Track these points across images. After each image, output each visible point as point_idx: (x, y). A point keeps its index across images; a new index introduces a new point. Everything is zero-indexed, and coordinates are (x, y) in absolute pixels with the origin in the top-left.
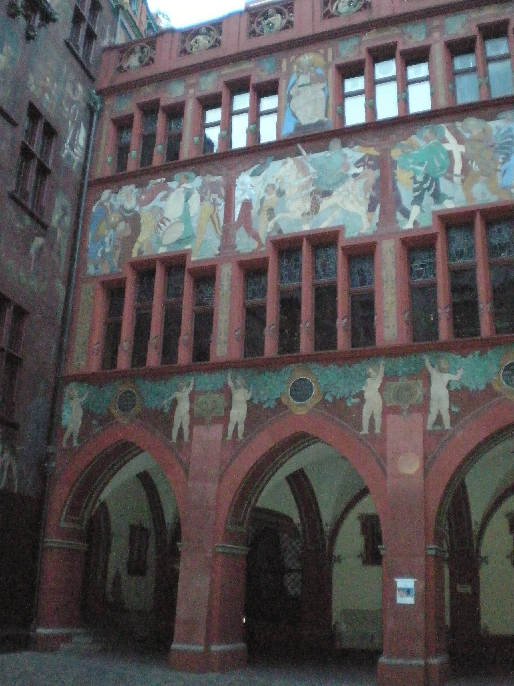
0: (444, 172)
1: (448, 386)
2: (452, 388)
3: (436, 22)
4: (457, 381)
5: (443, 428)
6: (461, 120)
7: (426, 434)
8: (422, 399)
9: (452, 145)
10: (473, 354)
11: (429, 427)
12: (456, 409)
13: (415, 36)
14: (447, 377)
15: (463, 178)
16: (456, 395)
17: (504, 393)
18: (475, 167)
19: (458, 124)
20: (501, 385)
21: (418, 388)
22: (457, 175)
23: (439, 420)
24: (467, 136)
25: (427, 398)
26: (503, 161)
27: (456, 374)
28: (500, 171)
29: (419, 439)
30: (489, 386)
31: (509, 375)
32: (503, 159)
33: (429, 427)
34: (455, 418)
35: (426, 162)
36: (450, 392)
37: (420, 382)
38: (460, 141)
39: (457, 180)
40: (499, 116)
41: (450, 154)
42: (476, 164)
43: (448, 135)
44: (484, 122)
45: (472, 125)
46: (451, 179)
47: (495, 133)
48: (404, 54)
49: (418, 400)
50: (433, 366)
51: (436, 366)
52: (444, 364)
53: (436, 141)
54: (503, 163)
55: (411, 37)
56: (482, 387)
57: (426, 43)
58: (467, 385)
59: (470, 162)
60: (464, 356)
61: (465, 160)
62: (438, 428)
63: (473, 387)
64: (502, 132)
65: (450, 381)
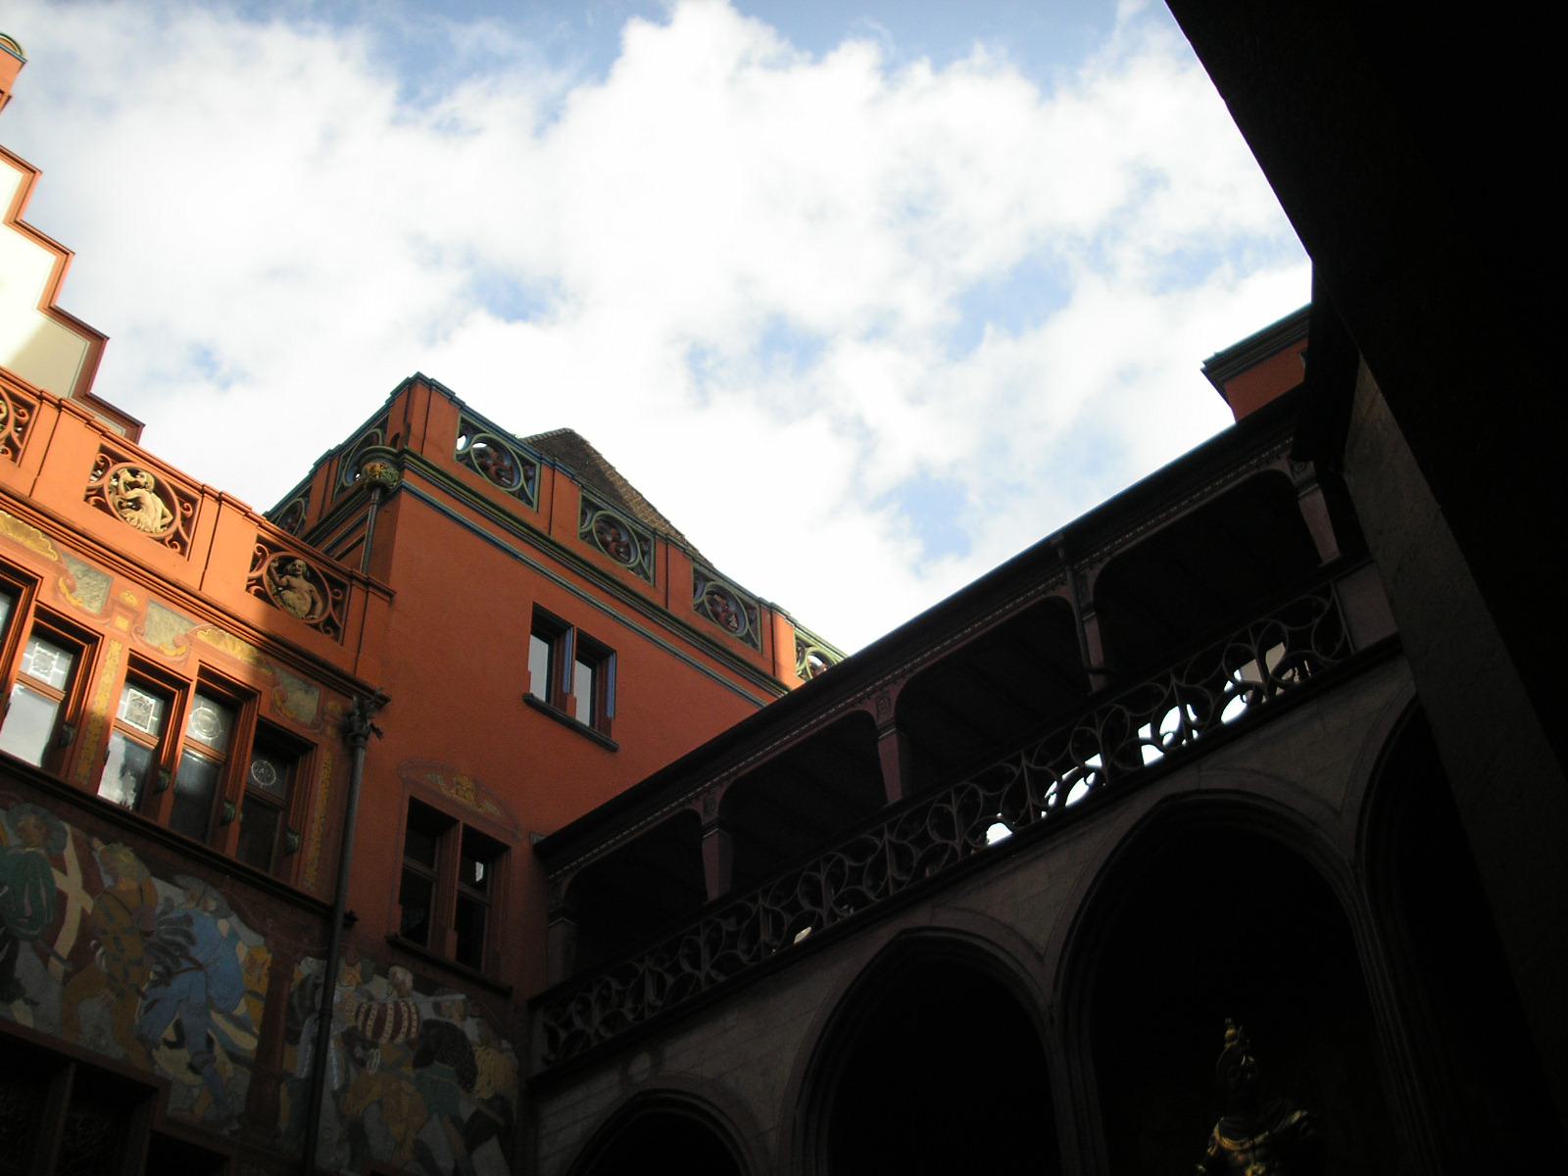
0: (36, 933)
3: (132, 595)
6: (106, 842)
9: (70, 882)
13: (80, 592)
15: (70, 969)
18: (100, 959)
19: (97, 844)
22: (59, 958)
24: (108, 881)
26: (156, 978)
28: (144, 997)
32: (156, 973)
35: (6, 888)
38: (91, 884)
39: (57, 968)
40: (180, 879)
41: (61, 899)
42: (103, 954)
43: (70, 853)
44: (147, 872)
45: (124, 863)
46: (46, 963)
47: (159, 910)
48: (42, 613)
53: (42, 852)
54: (155, 984)
55: (72, 589)
57: (94, 624)
59: (93, 942)
61: (86, 932)
64: (172, 915)
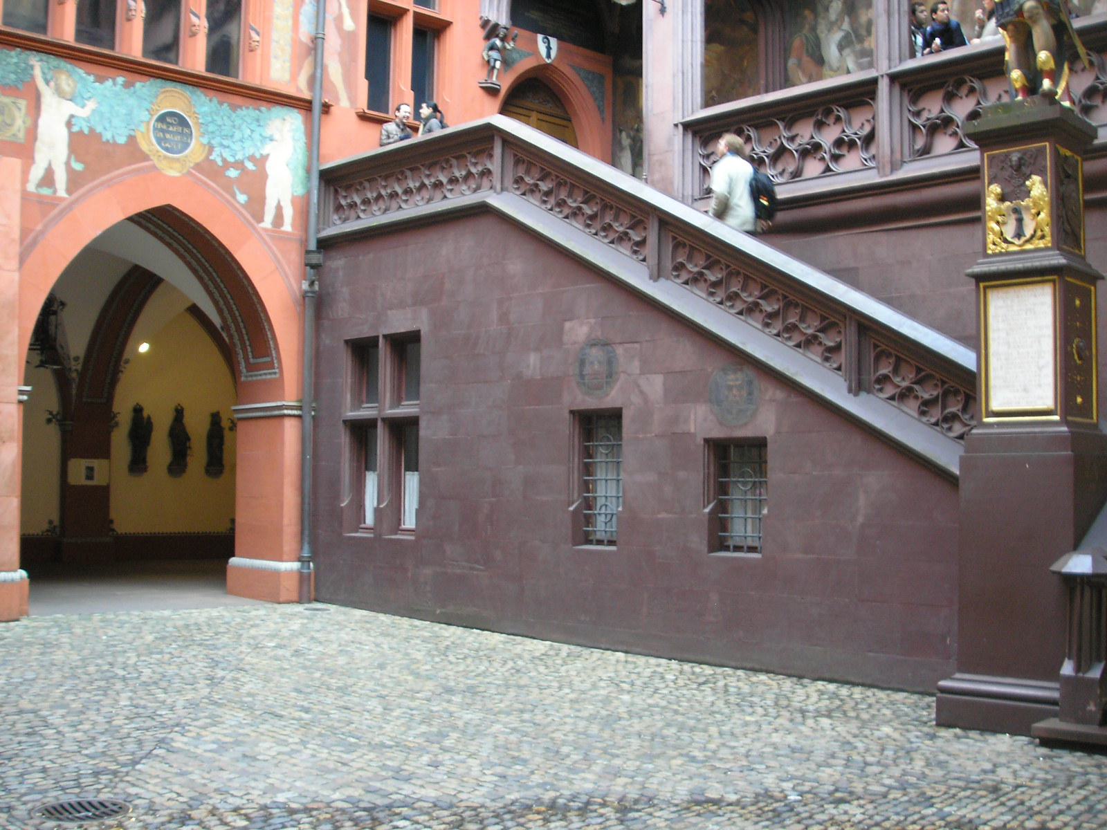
1: (69, 124)
2: (75, 129)
4: (84, 119)
5: (55, 191)
7: (25, 196)
8: (21, 135)
10: (114, 80)
11: (31, 187)
12: (78, 167)
14: (69, 108)
16: (83, 143)
17: (152, 157)
20: (150, 143)
21: (17, 113)
23: (48, 179)
25: (32, 134)
27: (83, 107)
29: (14, 204)
30: (132, 139)
31: (162, 130)
33: (31, 187)
34: (75, 181)
36: (71, 134)
37: (23, 103)
49: (14, 135)
50: (47, 82)
51: (52, 84)
52: (65, 82)
56: (122, 140)
58: (99, 129)
60: (100, 79)
62: (46, 191)
63: (107, 136)
65: (72, 116)
